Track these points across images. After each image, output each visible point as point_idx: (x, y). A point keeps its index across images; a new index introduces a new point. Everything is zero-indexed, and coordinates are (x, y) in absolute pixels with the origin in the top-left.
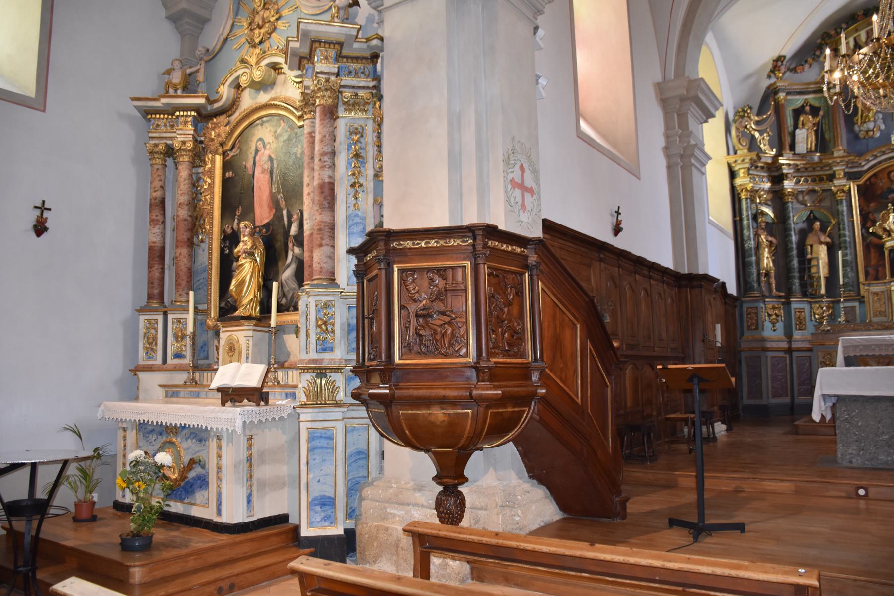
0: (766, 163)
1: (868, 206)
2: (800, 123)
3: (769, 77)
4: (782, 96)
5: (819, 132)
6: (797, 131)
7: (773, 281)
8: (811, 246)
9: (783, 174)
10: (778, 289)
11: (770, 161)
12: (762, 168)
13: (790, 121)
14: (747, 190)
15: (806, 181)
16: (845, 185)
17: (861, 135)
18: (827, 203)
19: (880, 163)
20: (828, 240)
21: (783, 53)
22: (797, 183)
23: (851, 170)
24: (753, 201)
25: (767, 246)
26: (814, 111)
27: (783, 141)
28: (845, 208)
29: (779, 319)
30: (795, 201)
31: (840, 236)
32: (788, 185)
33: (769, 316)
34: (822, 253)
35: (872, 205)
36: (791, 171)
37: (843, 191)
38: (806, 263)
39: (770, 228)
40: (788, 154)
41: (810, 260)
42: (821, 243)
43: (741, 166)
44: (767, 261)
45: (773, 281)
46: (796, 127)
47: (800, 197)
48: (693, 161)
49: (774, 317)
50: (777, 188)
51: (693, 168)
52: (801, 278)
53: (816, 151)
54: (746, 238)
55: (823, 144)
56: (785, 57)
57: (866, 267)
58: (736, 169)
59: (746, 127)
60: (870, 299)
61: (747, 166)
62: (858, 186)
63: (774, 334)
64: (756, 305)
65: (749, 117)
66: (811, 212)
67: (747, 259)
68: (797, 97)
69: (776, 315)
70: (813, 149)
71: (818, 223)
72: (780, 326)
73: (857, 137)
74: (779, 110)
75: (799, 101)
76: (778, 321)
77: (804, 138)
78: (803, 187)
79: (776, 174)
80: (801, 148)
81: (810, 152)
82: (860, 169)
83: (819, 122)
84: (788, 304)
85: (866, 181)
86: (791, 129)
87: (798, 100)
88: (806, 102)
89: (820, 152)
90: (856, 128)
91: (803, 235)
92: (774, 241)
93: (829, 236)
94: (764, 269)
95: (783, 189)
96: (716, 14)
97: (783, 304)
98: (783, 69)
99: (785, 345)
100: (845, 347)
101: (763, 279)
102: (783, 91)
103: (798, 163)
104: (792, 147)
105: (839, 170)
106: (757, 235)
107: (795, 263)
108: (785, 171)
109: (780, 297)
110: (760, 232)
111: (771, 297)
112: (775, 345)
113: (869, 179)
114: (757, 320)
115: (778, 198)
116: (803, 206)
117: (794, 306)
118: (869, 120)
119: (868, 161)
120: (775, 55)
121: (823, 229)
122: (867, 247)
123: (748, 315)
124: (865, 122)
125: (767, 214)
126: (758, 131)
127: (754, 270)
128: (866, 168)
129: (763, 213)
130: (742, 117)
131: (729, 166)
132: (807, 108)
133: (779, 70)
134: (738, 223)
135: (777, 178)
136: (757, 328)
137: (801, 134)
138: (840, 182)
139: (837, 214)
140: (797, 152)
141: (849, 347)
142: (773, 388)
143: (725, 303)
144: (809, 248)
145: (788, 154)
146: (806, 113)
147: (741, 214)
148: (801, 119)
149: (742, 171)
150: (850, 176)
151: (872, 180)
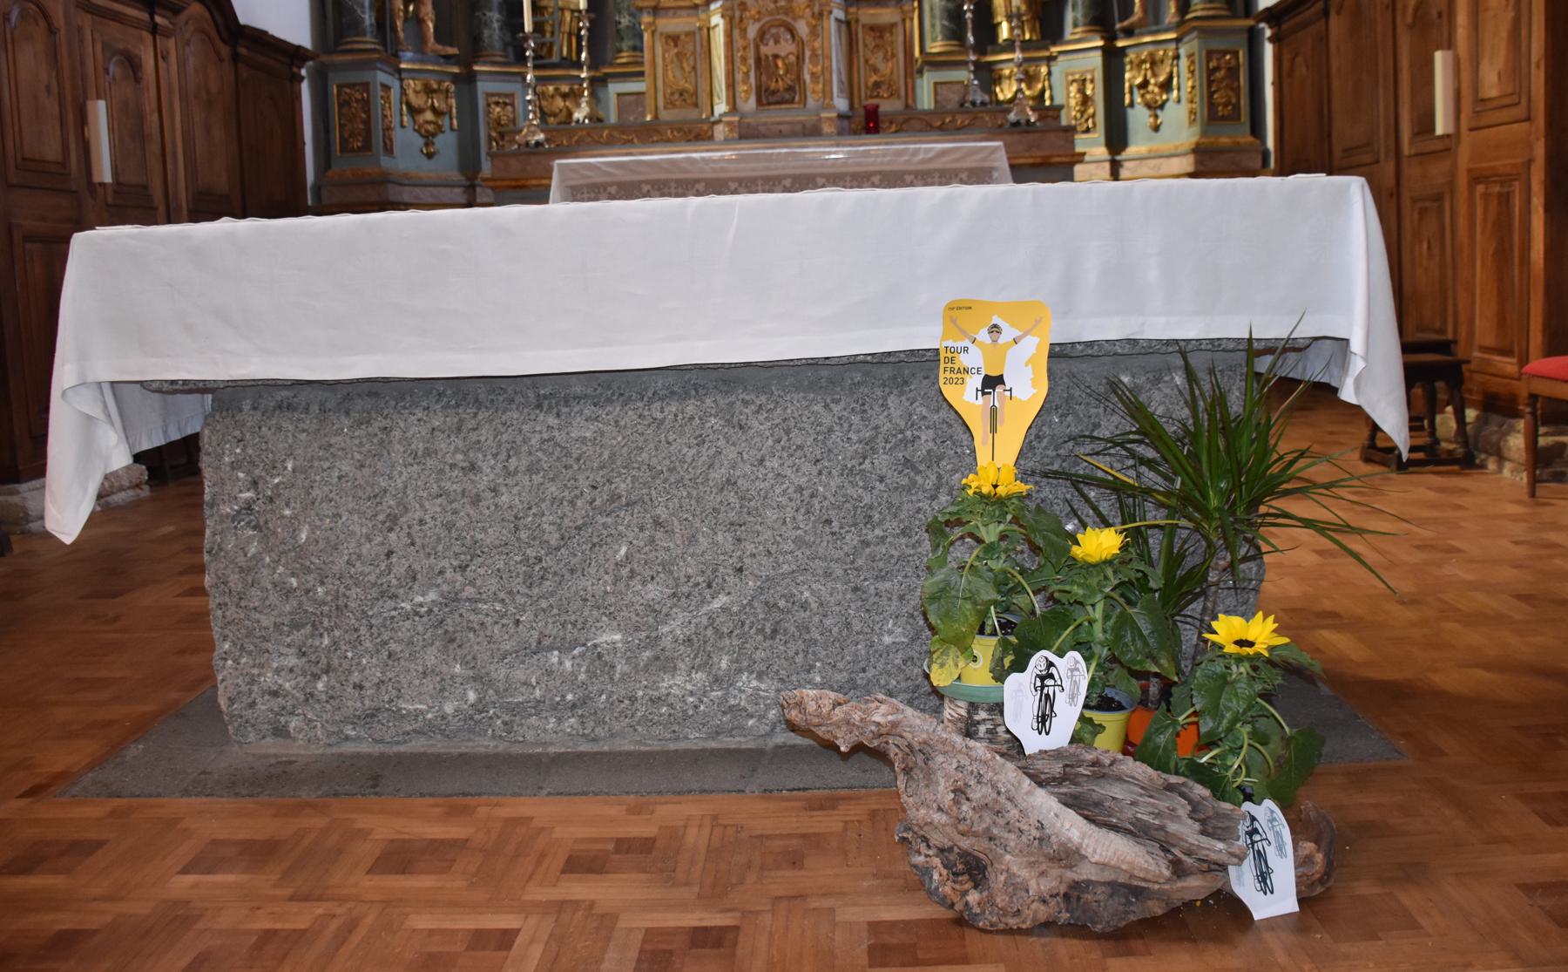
29: (445, 122)
33: (414, 111)
49: (429, 116)
64: (365, 76)
69: (433, 108)
72: (446, 143)
76: (440, 129)
84: (467, 80)
97: (455, 79)
109: (448, 58)
114: (367, 122)
117: (483, 87)
123: (341, 106)
136: (367, 146)
143: (235, 58)
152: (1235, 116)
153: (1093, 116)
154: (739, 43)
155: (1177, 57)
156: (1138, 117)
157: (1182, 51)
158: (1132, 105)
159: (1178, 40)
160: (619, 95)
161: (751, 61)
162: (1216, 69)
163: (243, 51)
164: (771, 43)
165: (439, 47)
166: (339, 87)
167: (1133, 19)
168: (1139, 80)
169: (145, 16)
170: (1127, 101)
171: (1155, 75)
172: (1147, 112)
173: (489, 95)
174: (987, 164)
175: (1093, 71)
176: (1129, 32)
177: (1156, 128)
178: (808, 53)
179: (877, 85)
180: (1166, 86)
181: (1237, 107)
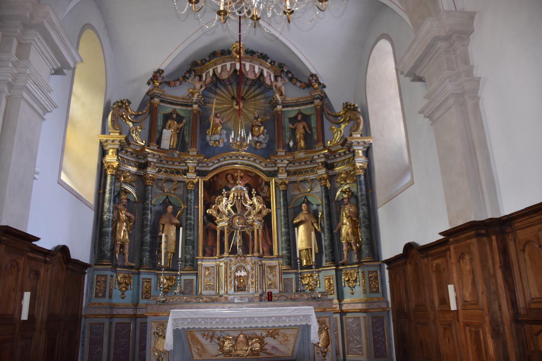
0: (135, 150)
1: (210, 199)
2: (168, 125)
3: (149, 83)
4: (156, 100)
5: (180, 134)
6: (165, 131)
8: (163, 225)
9: (148, 161)
10: (131, 259)
11: (138, 149)
12: (132, 154)
13: (160, 122)
16: (194, 179)
19: (221, 166)
20: (177, 221)
21: (162, 68)
22: (159, 171)
23: (201, 169)
25: (125, 221)
26: (179, 119)
27: (154, 137)
28: (193, 197)
30: (155, 186)
31: (187, 220)
32: (151, 171)
33: (120, 284)
36: (155, 160)
37: (193, 183)
39: (130, 206)
42: (172, 224)
43: (112, 147)
44: (123, 234)
45: (126, 251)
46: (164, 127)
48: (25, 95)
49: (124, 285)
50: (142, 173)
51: (23, 102)
53: (176, 149)
55: (182, 146)
56: (163, 71)
58: (107, 148)
59: (122, 116)
60: (202, 272)
61: (117, 147)
62: (204, 182)
63: (122, 301)
65: (127, 109)
66: (167, 197)
67: (104, 229)
68: (169, 106)
69: (125, 283)
70: (175, 146)
71: (171, 207)
73: (207, 144)
74: (153, 111)
75: (169, 108)
76: (127, 289)
77: (168, 138)
78: (162, 176)
79: (143, 161)
80: (166, 144)
82: (207, 169)
83: (182, 127)
85: (211, 179)
86: (160, 128)
87: (168, 108)
88: (175, 110)
89: (180, 151)
90: (208, 138)
91: (160, 214)
92: (133, 217)
93: (178, 218)
94: (120, 240)
95: (146, 174)
99: (130, 312)
100: (175, 320)
101: (118, 249)
102: (159, 97)
103: (161, 154)
104: (159, 142)
105: (191, 164)
107: (148, 238)
108: (150, 159)
109: (132, 267)
110: (120, 207)
111: (124, 267)
112: (120, 311)
113: (213, 177)
115: (141, 180)
116: (161, 192)
117: (142, 276)
118: (217, 133)
119: (214, 163)
121: (174, 213)
122: (206, 231)
123: (97, 282)
124: (214, 134)
125: (129, 193)
126: (132, 122)
128: (211, 169)
129: (126, 192)
130: (120, 107)
131: (101, 143)
132: (174, 116)
133: (157, 80)
134: (101, 195)
135: (143, 166)
138: (191, 175)
140: (162, 147)
141: (178, 319)
142: (115, 354)
143: (68, 269)
144: (162, 226)
146: (173, 119)
148: (169, 122)
150: (200, 173)
151: (215, 179)
152: (377, 291)
153: (333, 290)
154: (229, 271)
155: (358, 272)
156: (347, 290)
157: (360, 270)
158: (345, 286)
159: (358, 267)
160: (185, 280)
161: (233, 277)
162: (371, 277)
163: (70, 266)
164: (239, 272)
165: (129, 263)
166: (97, 276)
167: (344, 260)
168: (347, 279)
169: (43, 258)
170: (343, 285)
171: (352, 278)
172: (350, 289)
173: (143, 279)
174: (308, 314)
175: (332, 276)
176: (343, 264)
177: (353, 294)
178: (250, 275)
179: (271, 284)
180: (355, 281)
181: (378, 288)
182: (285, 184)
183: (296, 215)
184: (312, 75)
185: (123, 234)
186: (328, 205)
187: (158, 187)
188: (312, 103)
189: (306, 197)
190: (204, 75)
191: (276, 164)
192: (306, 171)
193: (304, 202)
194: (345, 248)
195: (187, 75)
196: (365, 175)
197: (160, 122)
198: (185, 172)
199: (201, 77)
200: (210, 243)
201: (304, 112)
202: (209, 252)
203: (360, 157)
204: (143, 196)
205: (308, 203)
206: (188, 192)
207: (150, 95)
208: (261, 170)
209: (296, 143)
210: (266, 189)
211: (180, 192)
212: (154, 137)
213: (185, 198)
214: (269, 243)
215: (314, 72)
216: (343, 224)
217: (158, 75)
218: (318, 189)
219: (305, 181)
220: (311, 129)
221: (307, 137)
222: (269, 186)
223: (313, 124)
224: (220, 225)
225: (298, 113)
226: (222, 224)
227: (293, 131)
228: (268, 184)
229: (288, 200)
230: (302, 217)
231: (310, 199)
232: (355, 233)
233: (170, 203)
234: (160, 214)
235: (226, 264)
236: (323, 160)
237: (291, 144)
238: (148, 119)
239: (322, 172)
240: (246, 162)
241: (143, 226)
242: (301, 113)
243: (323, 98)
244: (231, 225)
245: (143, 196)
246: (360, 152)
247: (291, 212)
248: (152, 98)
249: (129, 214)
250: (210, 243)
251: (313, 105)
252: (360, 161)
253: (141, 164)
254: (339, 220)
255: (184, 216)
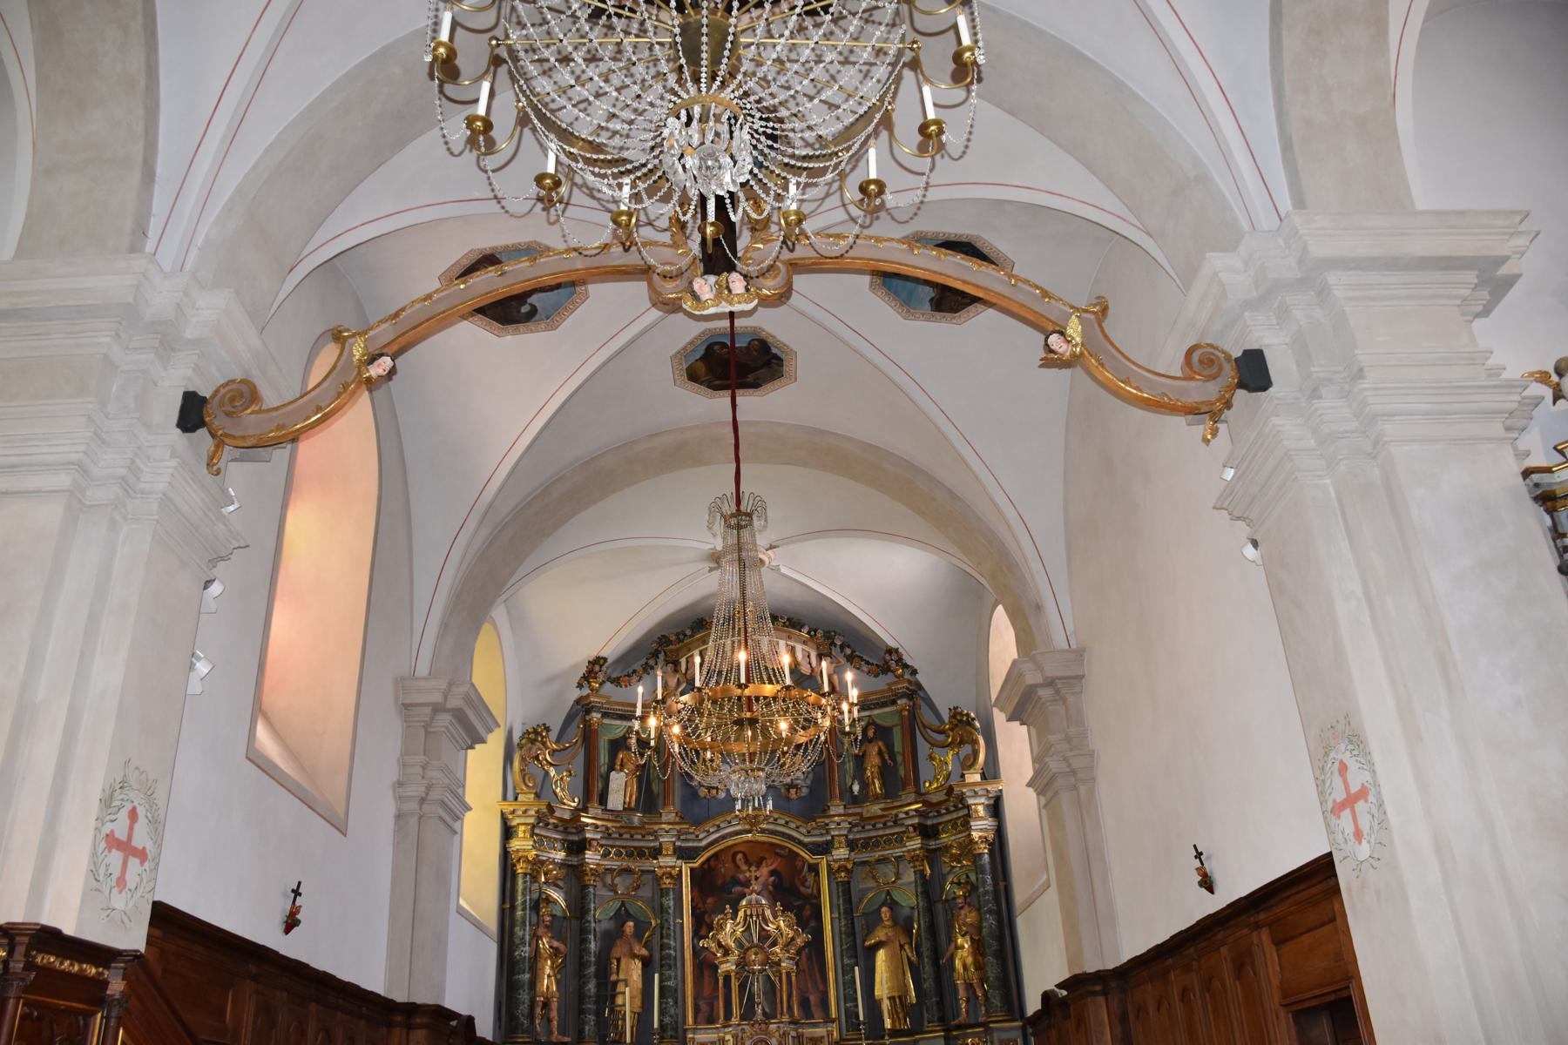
0: (561, 819)
3: (580, 686)
4: (596, 716)
6: (613, 774)
7: (554, 1014)
8: (619, 961)
10: (562, 1031)
11: (567, 816)
12: (556, 826)
13: (603, 757)
14: (527, 861)
15: (619, 854)
17: (703, 792)
18: (646, 892)
19: (724, 837)
20: (644, 952)
21: (603, 654)
22: (605, 856)
24: (535, 878)
25: (550, 957)
27: (593, 791)
28: (672, 903)
30: (599, 885)
32: (592, 857)
34: (634, 970)
35: (710, 900)
37: (670, 876)
38: (608, 990)
39: (556, 927)
40: (595, 810)
41: (615, 984)
42: (634, 956)
44: (547, 982)
45: (554, 1014)
46: (611, 768)
47: (608, 880)
52: (599, 1013)
53: (636, 809)
54: (517, 941)
56: (605, 659)
57: (696, 999)
58: (514, 823)
59: (537, 758)
61: (532, 820)
62: (692, 870)
65: (544, 744)
66: (623, 904)
68: (618, 722)
74: (589, 737)
77: (620, 788)
78: (615, 864)
79: (576, 838)
80: (616, 801)
81: (628, 809)
86: (603, 769)
87: (618, 727)
91: (611, 938)
92: (562, 947)
93: (645, 946)
95: (583, 864)
96: (512, 581)
98: (601, 677)
101: (538, 1011)
102: (598, 710)
103: (609, 825)
104: (603, 799)
106: (536, 937)
107: (591, 987)
108: (588, 835)
110: (541, 931)
113: (708, 860)
115: (574, 875)
119: (709, 833)
120: (592, 655)
121: (638, 934)
127: (524, 996)
128: (704, 843)
129: (549, 900)
130: (533, 742)
135: (577, 847)
137: (618, 780)
139: (662, 910)
140: (610, 806)
145: (595, 810)
147: (513, 900)
149: (522, 828)
150: (685, 854)
151: (712, 863)
176: (959, 1027)
182: (845, 869)
183: (869, 931)
184: (890, 651)
185: (547, 982)
186: (930, 910)
187: (604, 885)
188: (894, 702)
189: (888, 893)
190: (683, 661)
191: (828, 832)
192: (888, 841)
193: (884, 904)
194: (962, 993)
195: (651, 662)
196: (991, 853)
197: (603, 757)
198: (656, 853)
199: (676, 664)
200: (707, 992)
201: (878, 721)
202: (708, 1017)
203: (982, 818)
204: (579, 906)
205: (893, 905)
206: (664, 893)
207: (583, 707)
208: (800, 843)
209: (865, 786)
210: (811, 879)
211: (646, 892)
212: (593, 791)
213: (656, 904)
214: (821, 987)
215: (892, 644)
216: (957, 948)
217: (597, 668)
218: (909, 876)
219: (884, 860)
220: (893, 756)
221: (886, 772)
222: (817, 874)
223: (898, 747)
224: (723, 968)
225: (868, 724)
226: (728, 966)
227: (860, 760)
228: (814, 869)
229: (854, 900)
230: (880, 934)
231: (896, 896)
232: (979, 967)
233: (629, 916)
234: (611, 938)
235: (735, 1036)
236: (916, 821)
237: (856, 788)
238: (582, 751)
239: (915, 844)
240: (771, 827)
241: (582, 965)
242: (874, 723)
243: (915, 692)
244: (742, 963)
245: (579, 906)
246: (980, 808)
247: (859, 924)
248: (588, 711)
249: (556, 944)
250: (707, 992)
251: (893, 708)
252: (981, 827)
253: (573, 842)
254: (951, 939)
255: (656, 940)
